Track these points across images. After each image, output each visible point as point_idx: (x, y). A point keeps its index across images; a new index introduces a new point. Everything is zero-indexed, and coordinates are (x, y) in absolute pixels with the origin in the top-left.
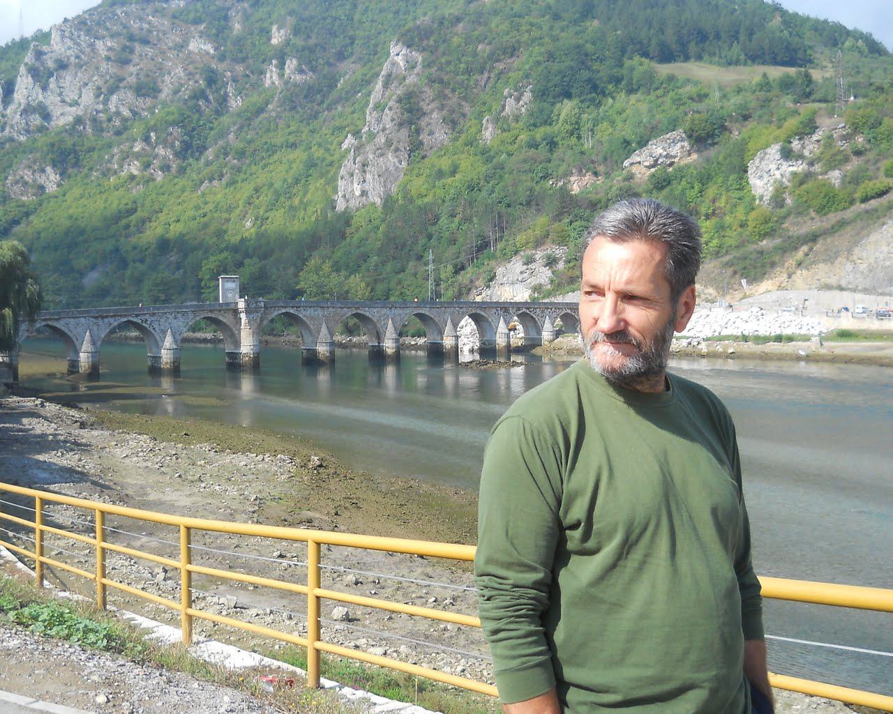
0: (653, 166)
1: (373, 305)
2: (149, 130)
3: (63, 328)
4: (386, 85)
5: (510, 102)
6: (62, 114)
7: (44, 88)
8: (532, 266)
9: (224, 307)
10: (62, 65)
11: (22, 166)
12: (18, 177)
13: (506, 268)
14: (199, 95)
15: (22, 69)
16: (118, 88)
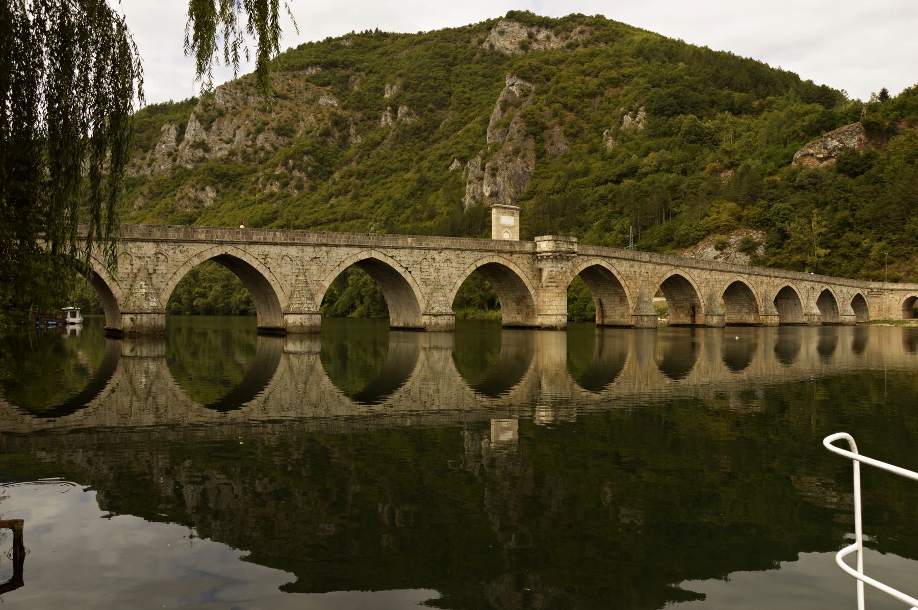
0: (826, 158)
1: (694, 265)
3: (255, 264)
4: (503, 110)
5: (628, 119)
6: (219, 149)
7: (208, 129)
8: (727, 251)
9: (517, 248)
10: (221, 114)
11: (188, 185)
12: (184, 194)
13: (694, 253)
14: (327, 133)
15: (192, 116)
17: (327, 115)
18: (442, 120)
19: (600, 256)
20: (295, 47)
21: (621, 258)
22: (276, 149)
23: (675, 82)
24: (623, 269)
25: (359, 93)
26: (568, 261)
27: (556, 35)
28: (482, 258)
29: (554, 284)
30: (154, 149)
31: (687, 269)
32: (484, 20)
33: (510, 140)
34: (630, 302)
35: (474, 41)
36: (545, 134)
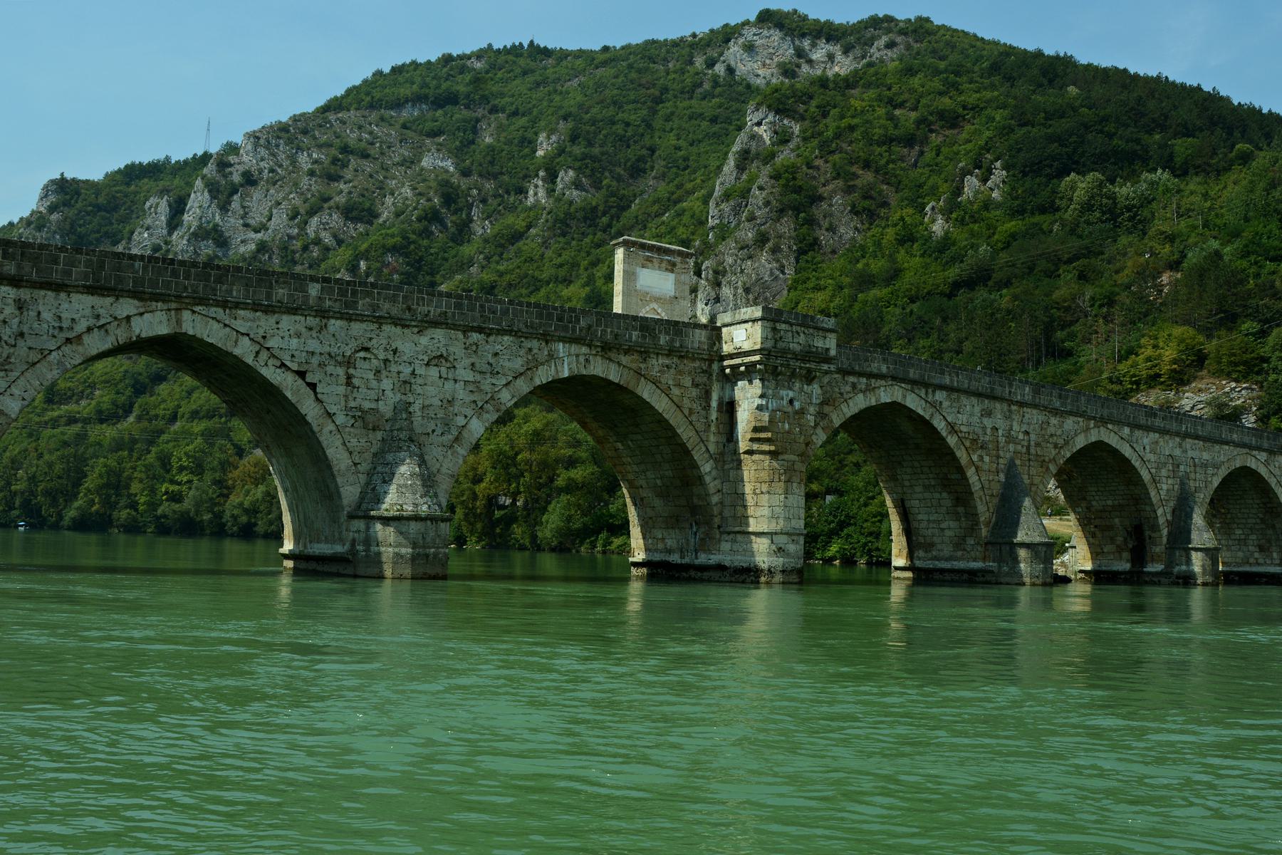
1: (1143, 422)
2: (357, 258)
4: (741, 168)
7: (224, 208)
10: (250, 180)
15: (199, 183)
16: (320, 209)
17: (433, 184)
18: (635, 196)
19: (903, 380)
20: (387, 70)
21: (957, 390)
22: (340, 242)
23: (1062, 117)
24: (963, 418)
25: (491, 148)
26: (809, 378)
27: (846, 52)
28: (552, 356)
29: (766, 447)
30: (130, 239)
31: (1127, 430)
32: (717, 25)
33: (751, 218)
34: (981, 508)
35: (699, 62)
36: (818, 211)
